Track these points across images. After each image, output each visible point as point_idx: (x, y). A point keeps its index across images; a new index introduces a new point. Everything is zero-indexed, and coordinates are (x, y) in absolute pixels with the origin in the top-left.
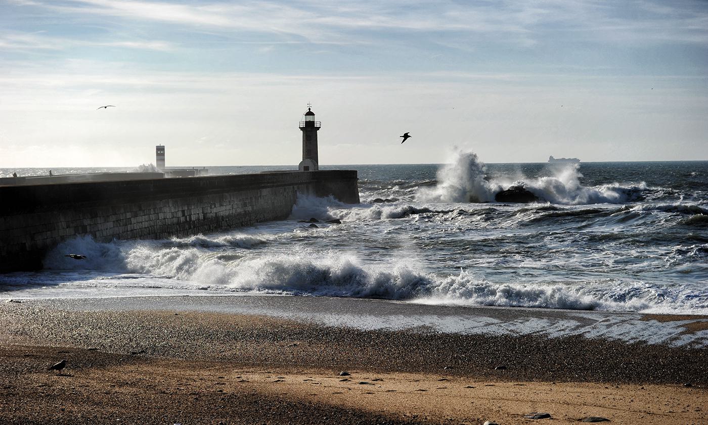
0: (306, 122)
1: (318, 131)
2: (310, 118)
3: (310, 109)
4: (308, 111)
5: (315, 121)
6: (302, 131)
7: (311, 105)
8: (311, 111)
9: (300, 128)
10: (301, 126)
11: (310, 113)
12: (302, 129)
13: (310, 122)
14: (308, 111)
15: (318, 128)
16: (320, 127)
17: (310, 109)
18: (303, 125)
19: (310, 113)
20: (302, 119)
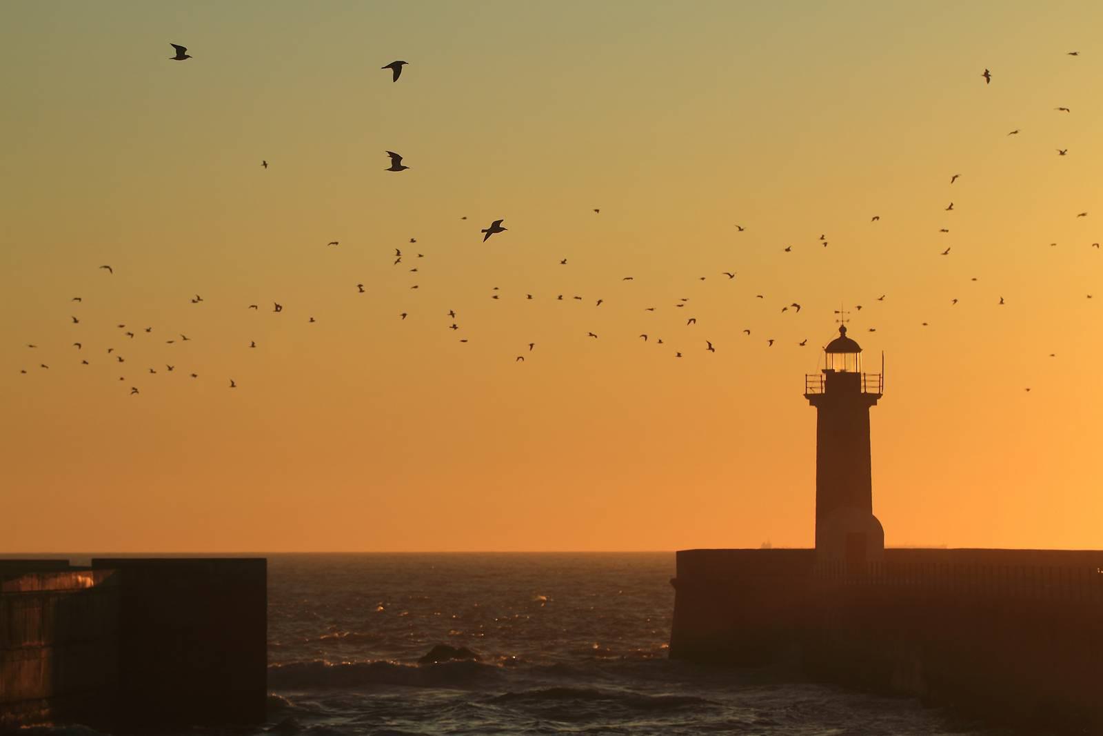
2: (840, 363)
3: (843, 330)
4: (838, 335)
5: (862, 373)
6: (814, 409)
7: (846, 317)
8: (848, 335)
9: (807, 396)
10: (809, 392)
11: (843, 345)
12: (813, 399)
14: (838, 335)
15: (873, 399)
16: (879, 396)
17: (843, 330)
18: (818, 389)
19: (843, 345)
20: (815, 365)
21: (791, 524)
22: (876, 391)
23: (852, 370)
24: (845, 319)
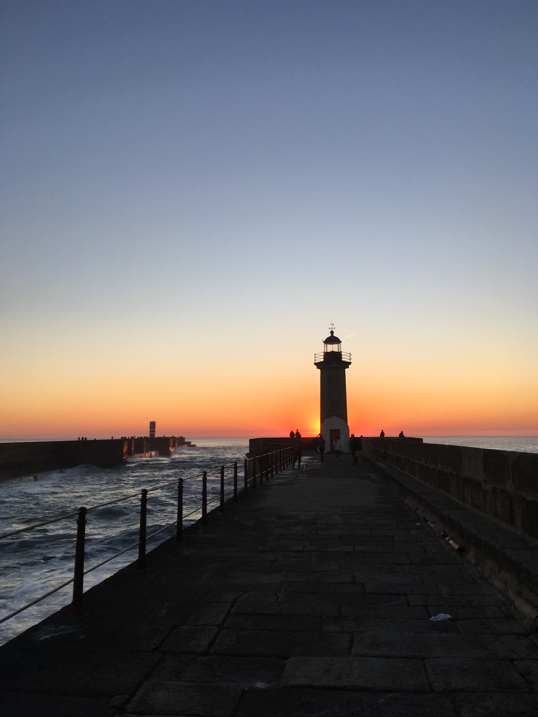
0: (327, 355)
1: (346, 370)
3: (332, 332)
6: (319, 370)
7: (333, 327)
8: (334, 335)
9: (315, 364)
10: (316, 362)
11: (332, 340)
13: (333, 352)
14: (330, 335)
15: (347, 364)
16: (350, 363)
17: (332, 332)
19: (332, 340)
20: (319, 350)
22: (349, 361)
24: (333, 327)
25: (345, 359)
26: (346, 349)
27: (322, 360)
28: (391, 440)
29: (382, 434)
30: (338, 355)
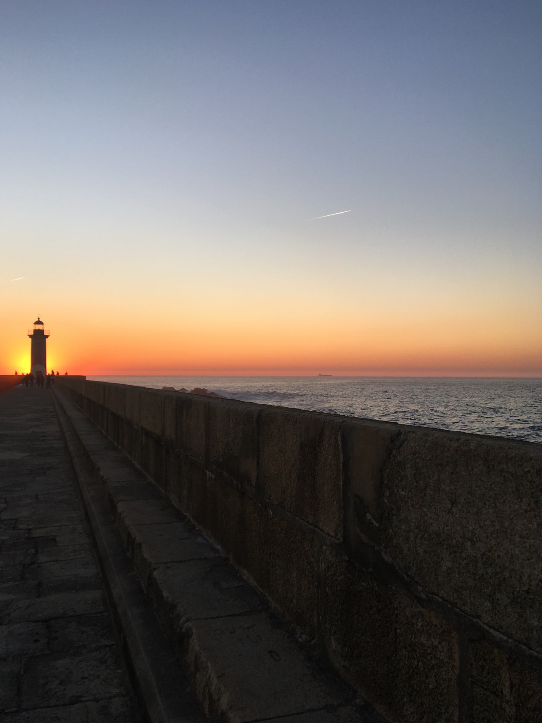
0: (35, 331)
1: (47, 339)
3: (39, 318)
6: (30, 339)
11: (39, 322)
12: (30, 336)
13: (39, 330)
14: (37, 320)
17: (39, 318)
19: (39, 322)
20: (31, 328)
21: (24, 365)
23: (41, 329)
25: (45, 334)
26: (47, 329)
27: (32, 334)
28: (62, 377)
29: (66, 374)
30: (42, 331)
